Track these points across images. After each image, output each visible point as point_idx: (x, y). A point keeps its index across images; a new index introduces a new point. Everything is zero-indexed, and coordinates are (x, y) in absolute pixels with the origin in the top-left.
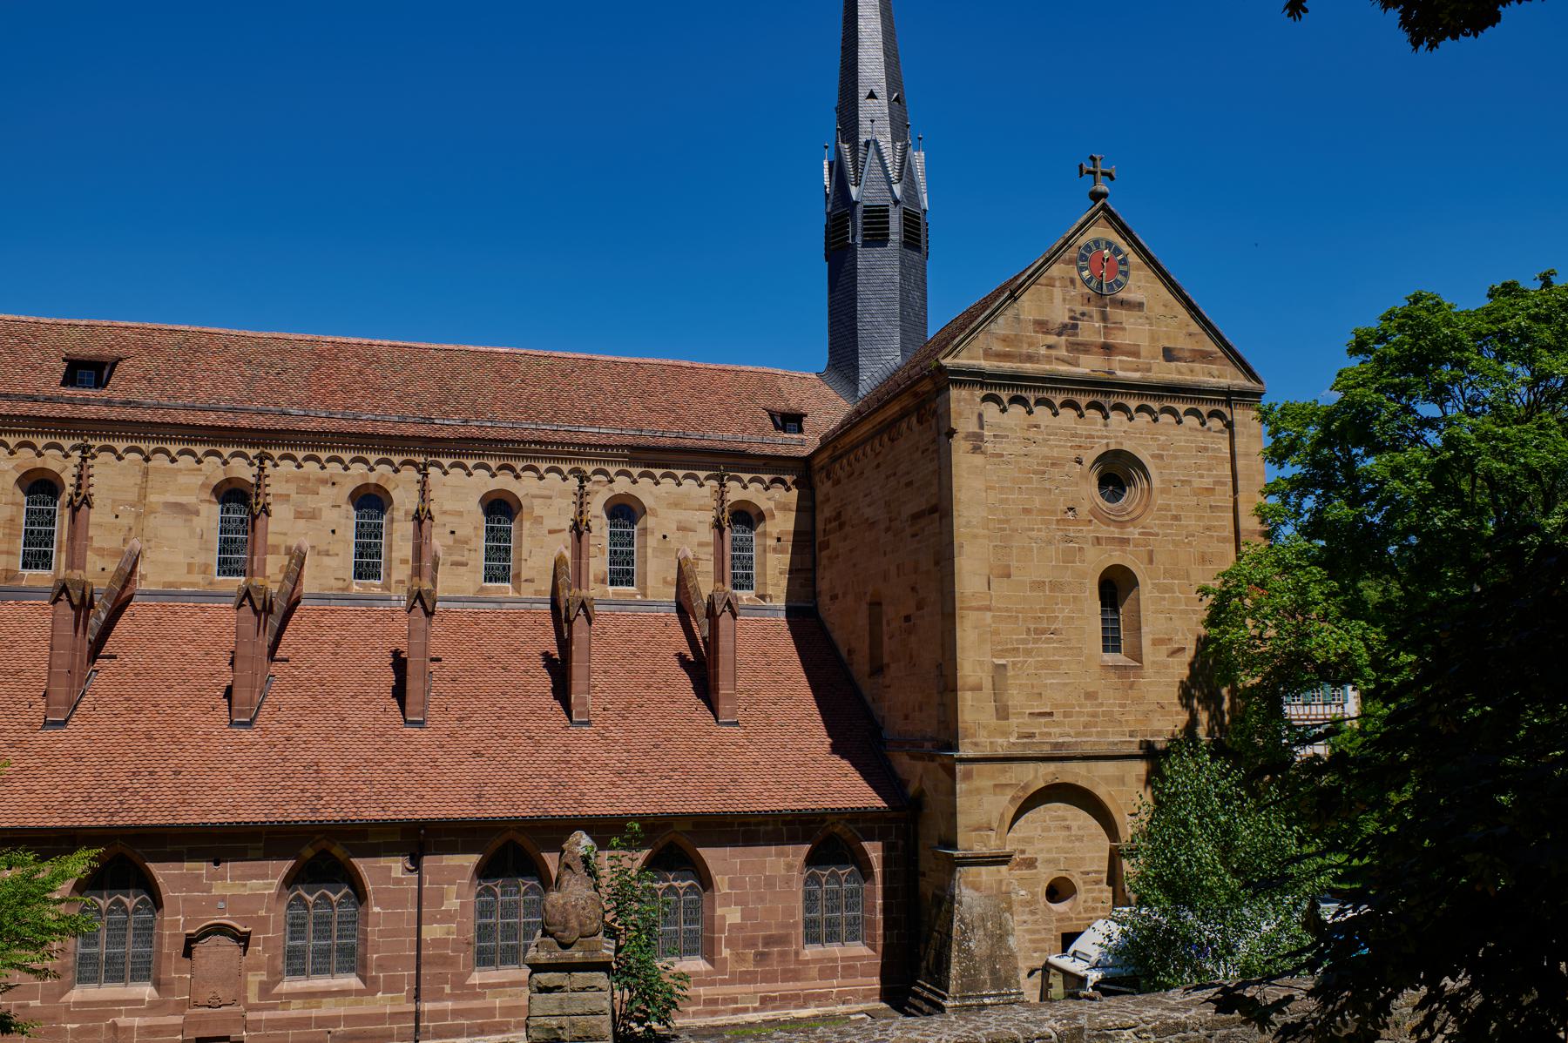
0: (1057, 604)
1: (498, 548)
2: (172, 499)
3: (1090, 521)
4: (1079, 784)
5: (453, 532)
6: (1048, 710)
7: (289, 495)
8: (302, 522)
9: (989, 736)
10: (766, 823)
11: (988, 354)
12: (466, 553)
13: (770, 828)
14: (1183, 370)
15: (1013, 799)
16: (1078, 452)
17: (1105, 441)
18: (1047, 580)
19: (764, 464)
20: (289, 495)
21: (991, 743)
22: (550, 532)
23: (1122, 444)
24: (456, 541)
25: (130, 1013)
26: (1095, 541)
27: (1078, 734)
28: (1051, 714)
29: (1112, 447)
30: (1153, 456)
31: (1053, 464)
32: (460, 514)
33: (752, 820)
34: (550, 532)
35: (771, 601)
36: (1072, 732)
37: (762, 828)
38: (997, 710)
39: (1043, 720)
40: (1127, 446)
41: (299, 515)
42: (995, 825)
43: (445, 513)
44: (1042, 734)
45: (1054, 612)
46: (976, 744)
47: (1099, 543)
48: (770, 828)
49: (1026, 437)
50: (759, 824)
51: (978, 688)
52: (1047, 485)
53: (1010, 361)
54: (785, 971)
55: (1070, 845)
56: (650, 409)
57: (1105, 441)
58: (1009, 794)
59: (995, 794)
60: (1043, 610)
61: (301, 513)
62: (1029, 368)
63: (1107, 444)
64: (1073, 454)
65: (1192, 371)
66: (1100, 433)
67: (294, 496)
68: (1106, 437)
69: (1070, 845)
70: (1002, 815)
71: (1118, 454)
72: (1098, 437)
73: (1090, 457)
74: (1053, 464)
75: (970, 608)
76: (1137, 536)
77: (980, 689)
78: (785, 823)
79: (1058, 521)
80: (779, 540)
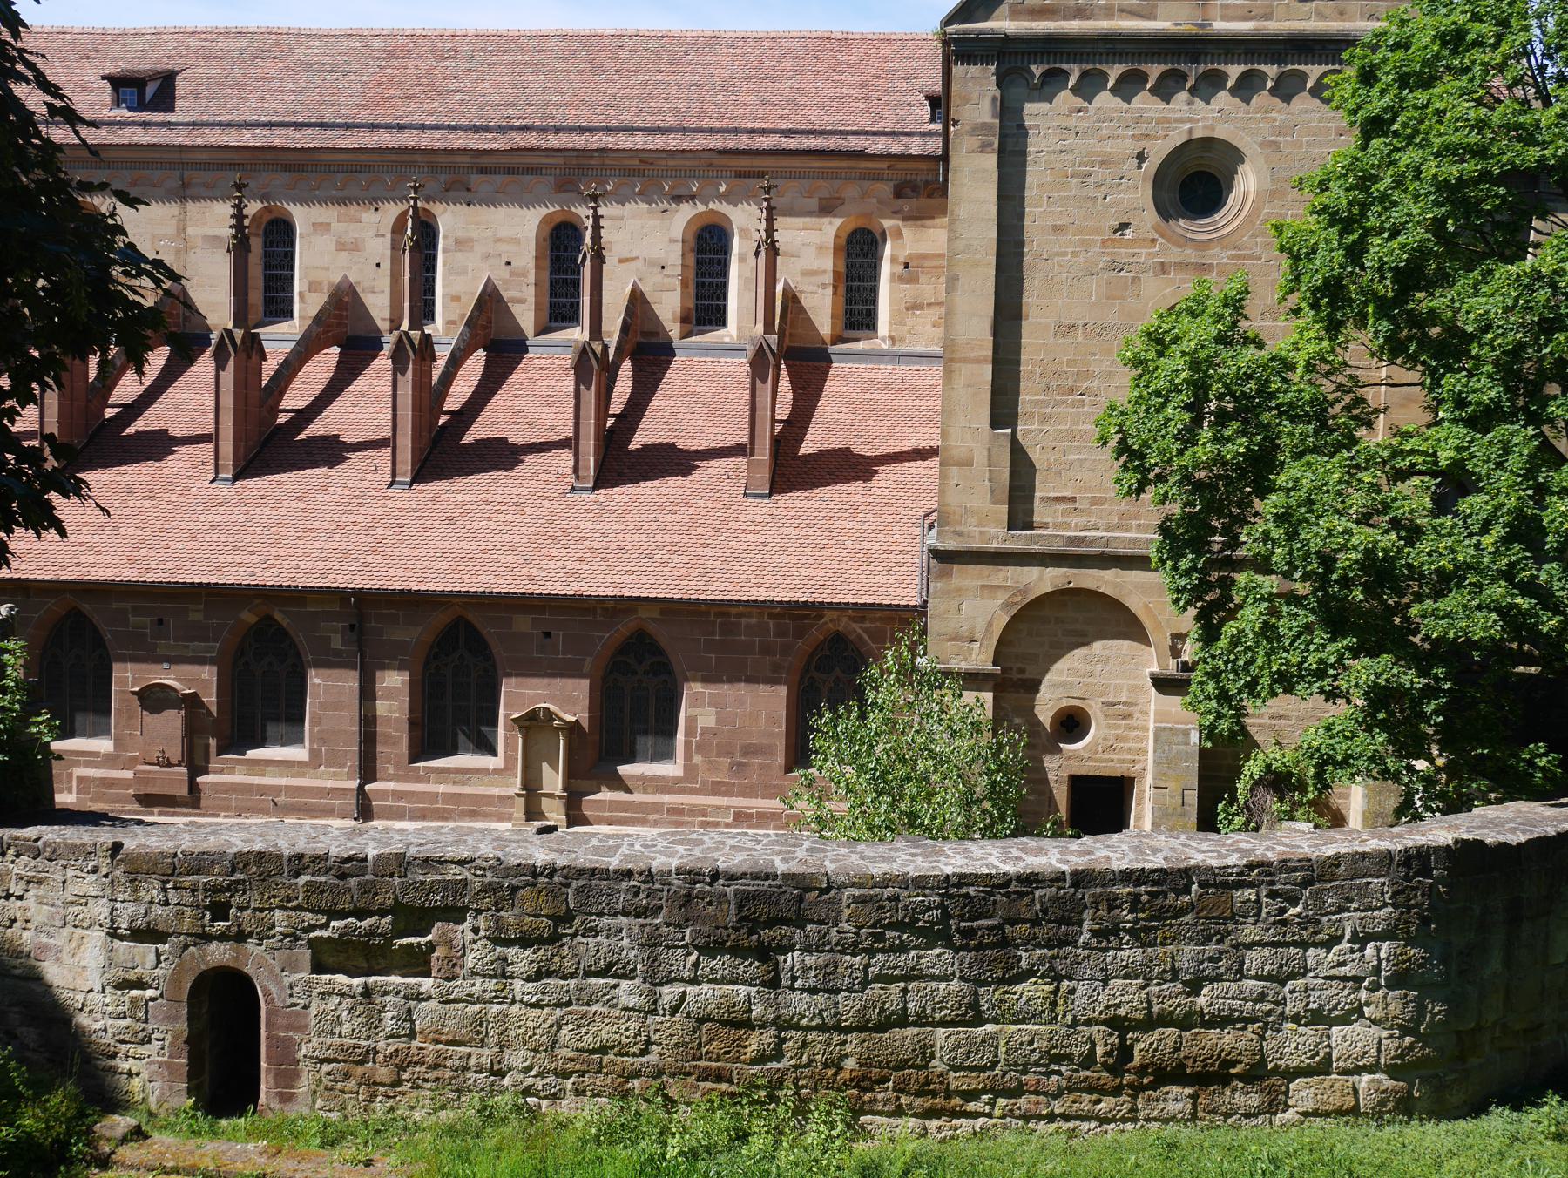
0: (1094, 354)
1: (565, 281)
2: (211, 232)
3: (1154, 241)
4: (1101, 590)
5: (509, 263)
6: (1068, 494)
7: (329, 224)
8: (344, 254)
9: (980, 525)
10: (750, 616)
11: (1015, 14)
12: (524, 287)
13: (754, 620)
14: (1328, 12)
15: (1006, 605)
16: (1143, 144)
17: (1188, 126)
18: (1081, 322)
19: (889, 167)
20: (329, 224)
21: (981, 533)
22: (621, 261)
23: (1213, 129)
24: (512, 274)
25: (88, 765)
26: (1158, 268)
27: (1109, 528)
28: (1073, 499)
29: (1198, 134)
30: (1262, 145)
31: (1103, 163)
32: (515, 241)
33: (734, 610)
34: (621, 261)
35: (893, 344)
36: (1102, 524)
37: (744, 621)
38: (992, 491)
39: (1060, 507)
40: (1221, 132)
41: (341, 247)
42: (978, 636)
43: (499, 240)
44: (1057, 526)
45: (1088, 364)
46: (960, 534)
47: (1164, 272)
48: (754, 620)
49: (1064, 124)
50: (740, 615)
51: (968, 463)
52: (1091, 192)
53: (1047, 19)
54: (765, 786)
55: (1088, 668)
56: (764, 101)
57: (1188, 126)
58: (1002, 597)
59: (982, 597)
60: (1070, 363)
61: (343, 244)
62: (1074, 26)
63: (1190, 131)
64: (1132, 147)
65: (1341, 14)
66: (1178, 115)
67: (335, 225)
68: (1190, 120)
69: (1088, 668)
70: (990, 624)
71: (1208, 143)
72: (1176, 121)
73: (1158, 152)
74: (1103, 163)
75: (965, 360)
76: (1224, 260)
77: (968, 463)
78: (771, 616)
79: (1104, 242)
80: (907, 266)
